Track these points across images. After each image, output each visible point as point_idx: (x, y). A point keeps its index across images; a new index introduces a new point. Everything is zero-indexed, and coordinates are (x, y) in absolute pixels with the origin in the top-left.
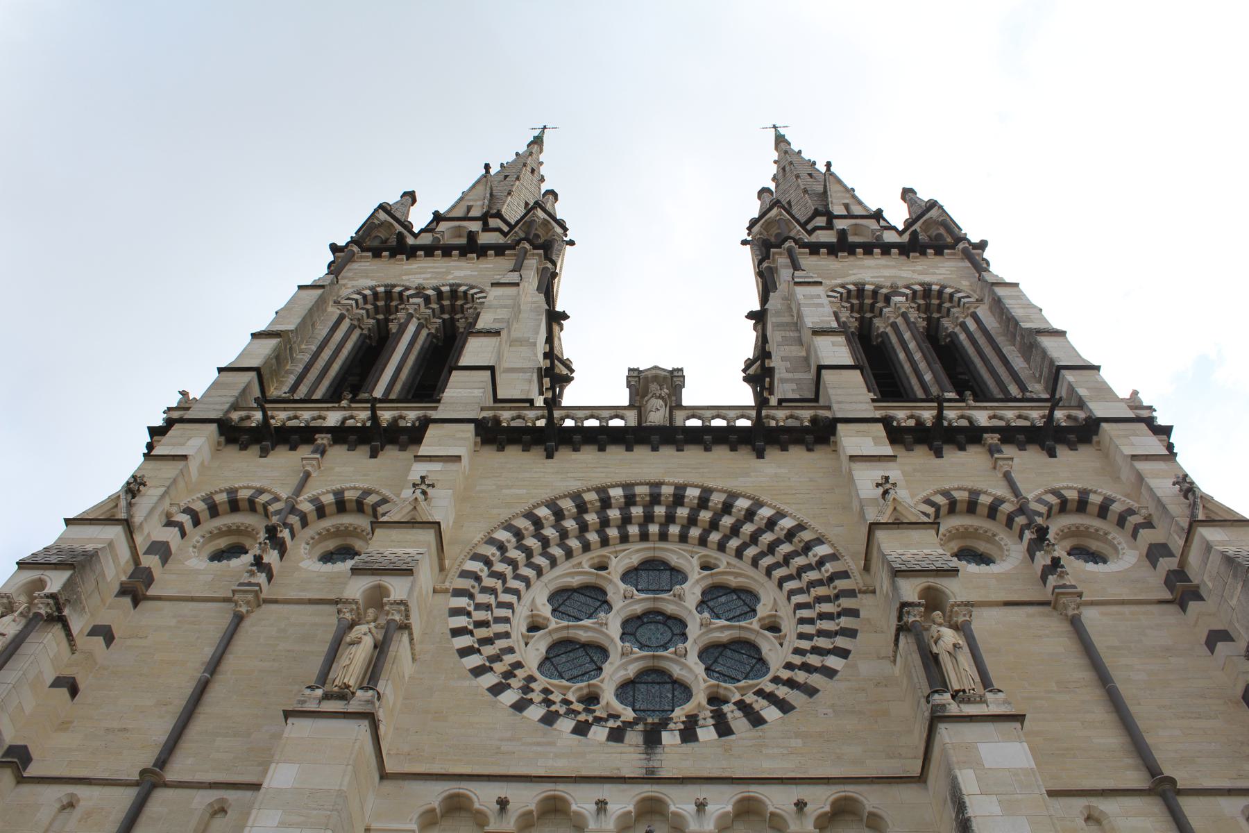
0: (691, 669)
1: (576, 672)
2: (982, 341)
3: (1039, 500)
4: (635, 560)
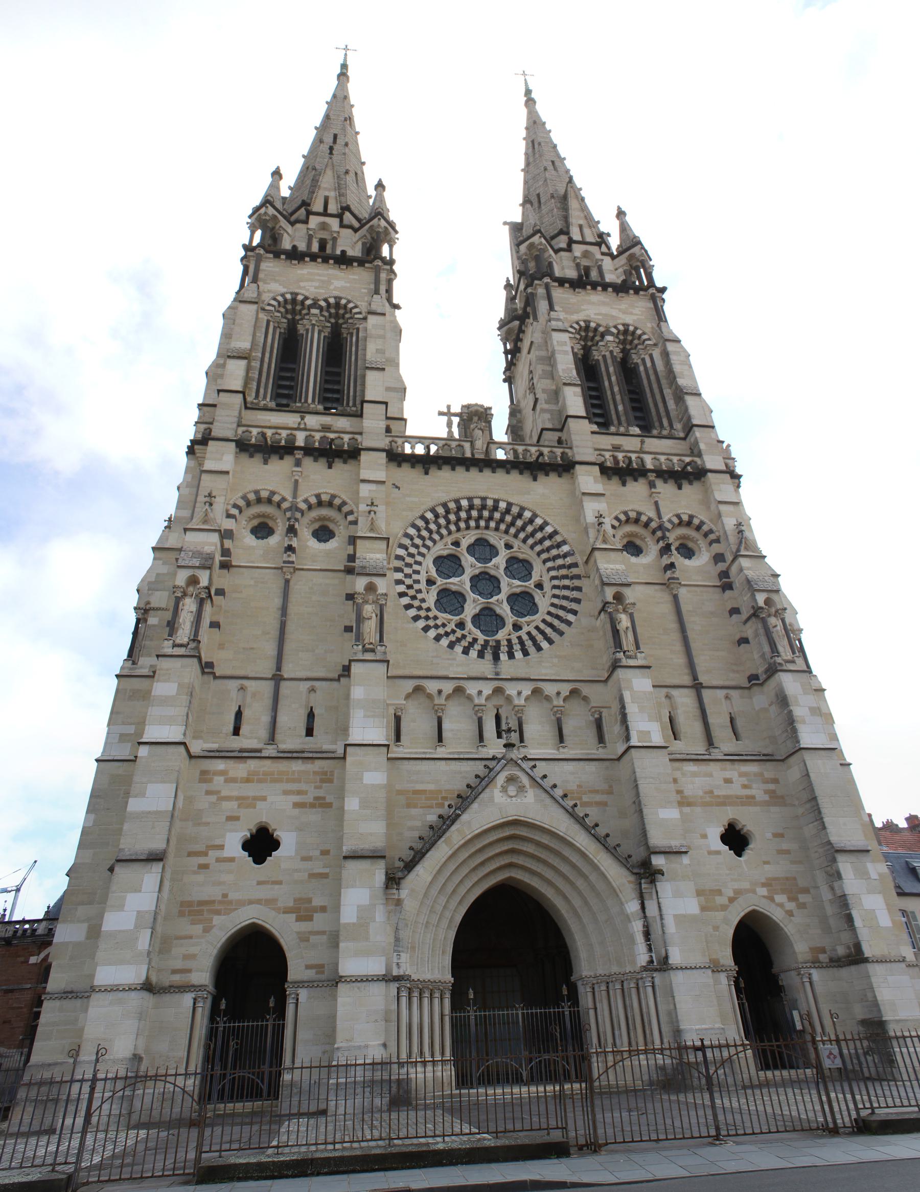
0: (505, 610)
2: (653, 378)
3: (670, 521)
4: (472, 540)
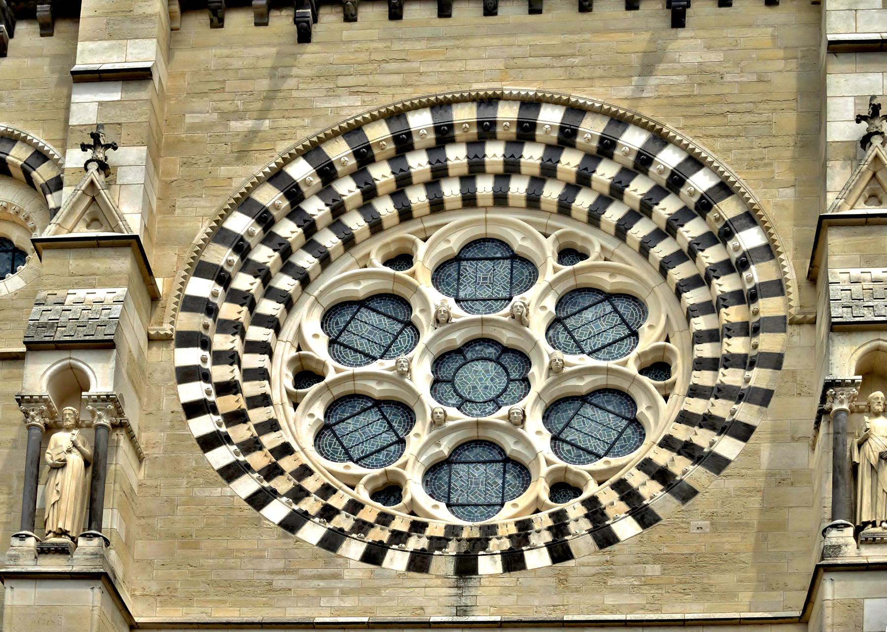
1: (369, 448)
